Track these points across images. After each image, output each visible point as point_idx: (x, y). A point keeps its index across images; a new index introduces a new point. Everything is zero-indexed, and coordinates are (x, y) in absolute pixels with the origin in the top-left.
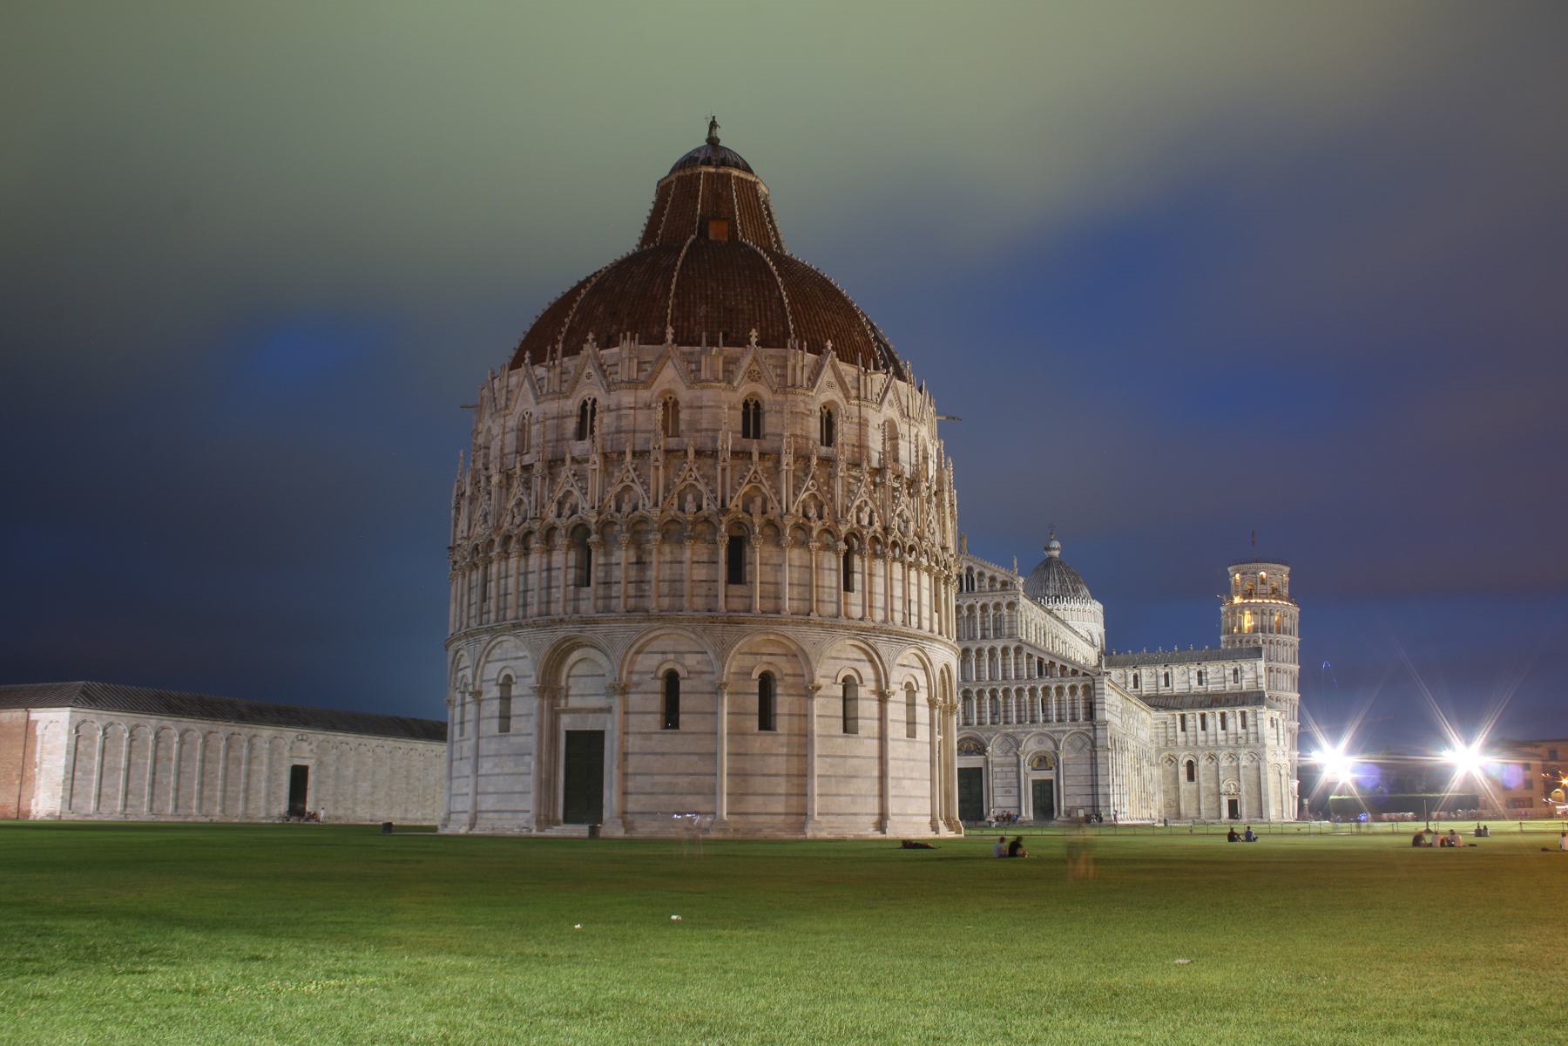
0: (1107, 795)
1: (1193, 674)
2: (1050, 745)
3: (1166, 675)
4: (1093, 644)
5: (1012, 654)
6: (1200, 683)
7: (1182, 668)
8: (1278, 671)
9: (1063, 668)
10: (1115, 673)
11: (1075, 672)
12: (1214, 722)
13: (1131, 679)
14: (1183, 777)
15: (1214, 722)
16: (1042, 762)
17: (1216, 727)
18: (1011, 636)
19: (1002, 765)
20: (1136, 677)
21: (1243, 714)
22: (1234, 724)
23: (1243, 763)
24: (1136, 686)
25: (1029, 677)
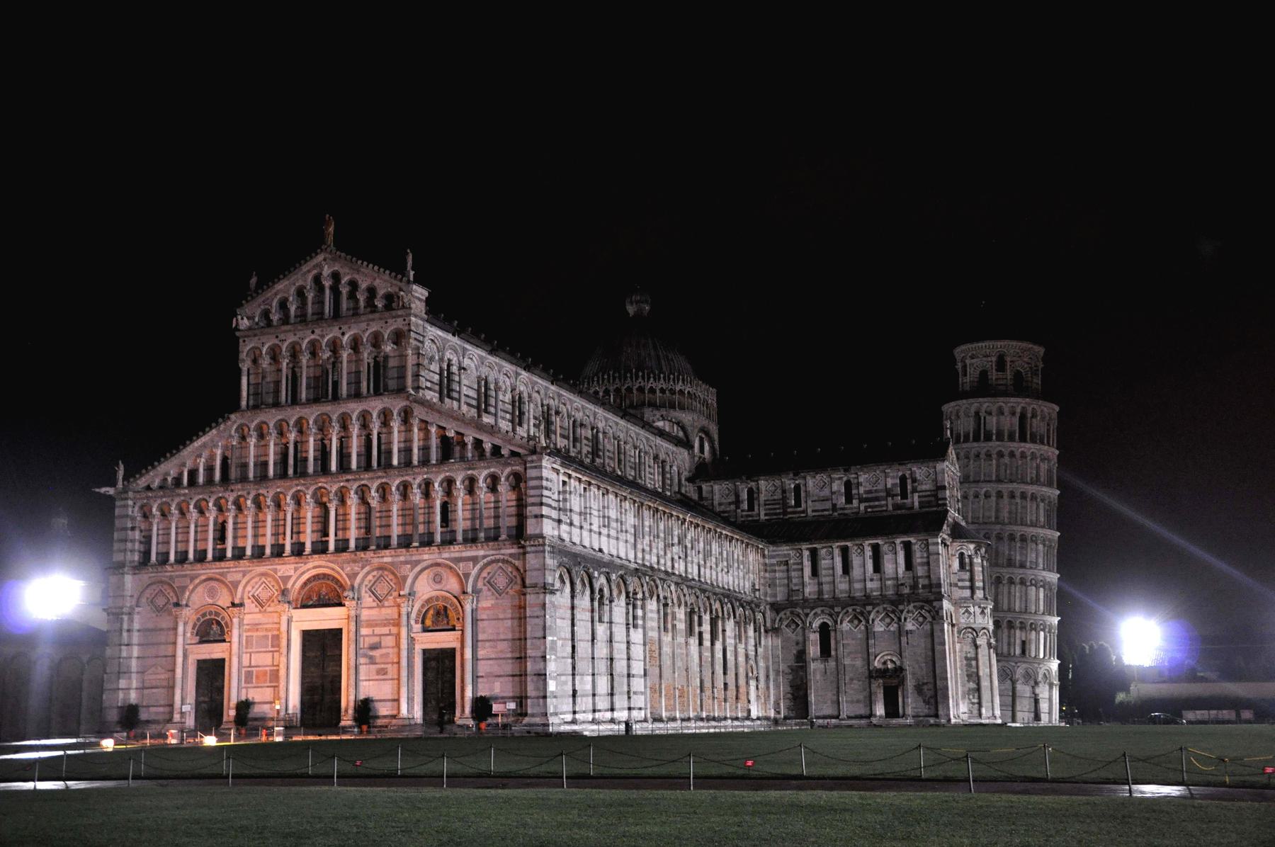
0: (542, 676)
1: (838, 486)
2: (453, 584)
3: (797, 488)
4: (686, 444)
5: (396, 425)
6: (849, 499)
7: (822, 477)
8: (1023, 496)
9: (478, 443)
10: (718, 491)
11: (496, 450)
12: (862, 562)
13: (745, 496)
14: (814, 650)
15: (862, 562)
16: (439, 617)
17: (867, 568)
18: (401, 390)
19: (372, 624)
20: (750, 492)
21: (908, 547)
22: (894, 564)
23: (909, 626)
24: (751, 508)
25: (425, 462)
